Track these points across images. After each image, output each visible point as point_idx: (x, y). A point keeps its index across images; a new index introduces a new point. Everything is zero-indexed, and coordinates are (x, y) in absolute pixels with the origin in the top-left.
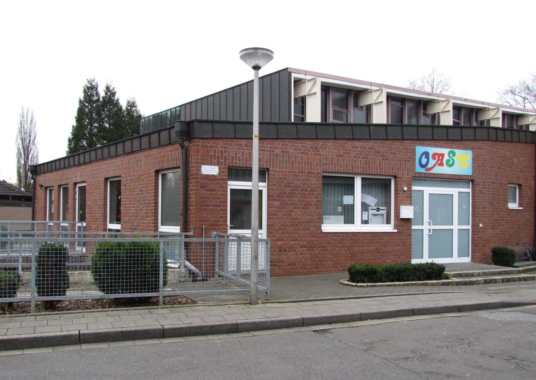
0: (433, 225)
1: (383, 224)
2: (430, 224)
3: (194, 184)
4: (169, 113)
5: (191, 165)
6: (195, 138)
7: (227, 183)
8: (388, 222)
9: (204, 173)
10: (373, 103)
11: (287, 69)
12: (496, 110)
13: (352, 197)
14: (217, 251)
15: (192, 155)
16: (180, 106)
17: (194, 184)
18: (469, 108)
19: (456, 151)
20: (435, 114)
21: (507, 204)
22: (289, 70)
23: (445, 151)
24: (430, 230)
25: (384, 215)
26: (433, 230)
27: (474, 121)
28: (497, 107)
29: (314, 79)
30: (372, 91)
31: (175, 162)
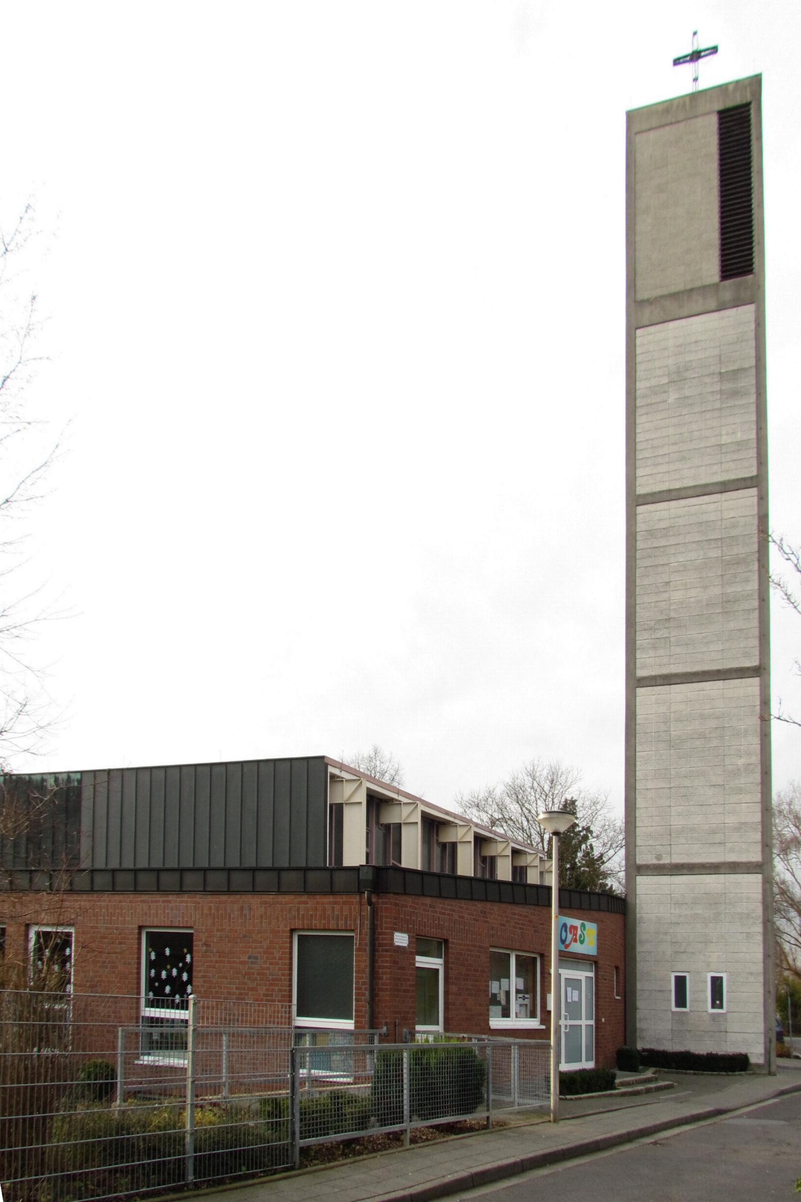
0: (570, 1019)
1: (526, 1017)
2: (566, 1019)
3: (388, 959)
4: (51, 781)
5: (379, 930)
6: (390, 893)
7: (414, 959)
8: (533, 1015)
9: (396, 944)
10: (458, 841)
11: (323, 758)
12: (506, 844)
13: (507, 980)
14: (362, 1085)
15: (382, 916)
16: (82, 772)
17: (388, 959)
18: (429, 819)
19: (586, 923)
20: (522, 867)
21: (488, 1020)
22: (326, 761)
23: (577, 923)
24: (566, 1026)
25: (529, 1007)
26: (570, 1026)
27: (374, 823)
28: (411, 801)
29: (360, 780)
30: (343, 781)
31: (306, 922)
